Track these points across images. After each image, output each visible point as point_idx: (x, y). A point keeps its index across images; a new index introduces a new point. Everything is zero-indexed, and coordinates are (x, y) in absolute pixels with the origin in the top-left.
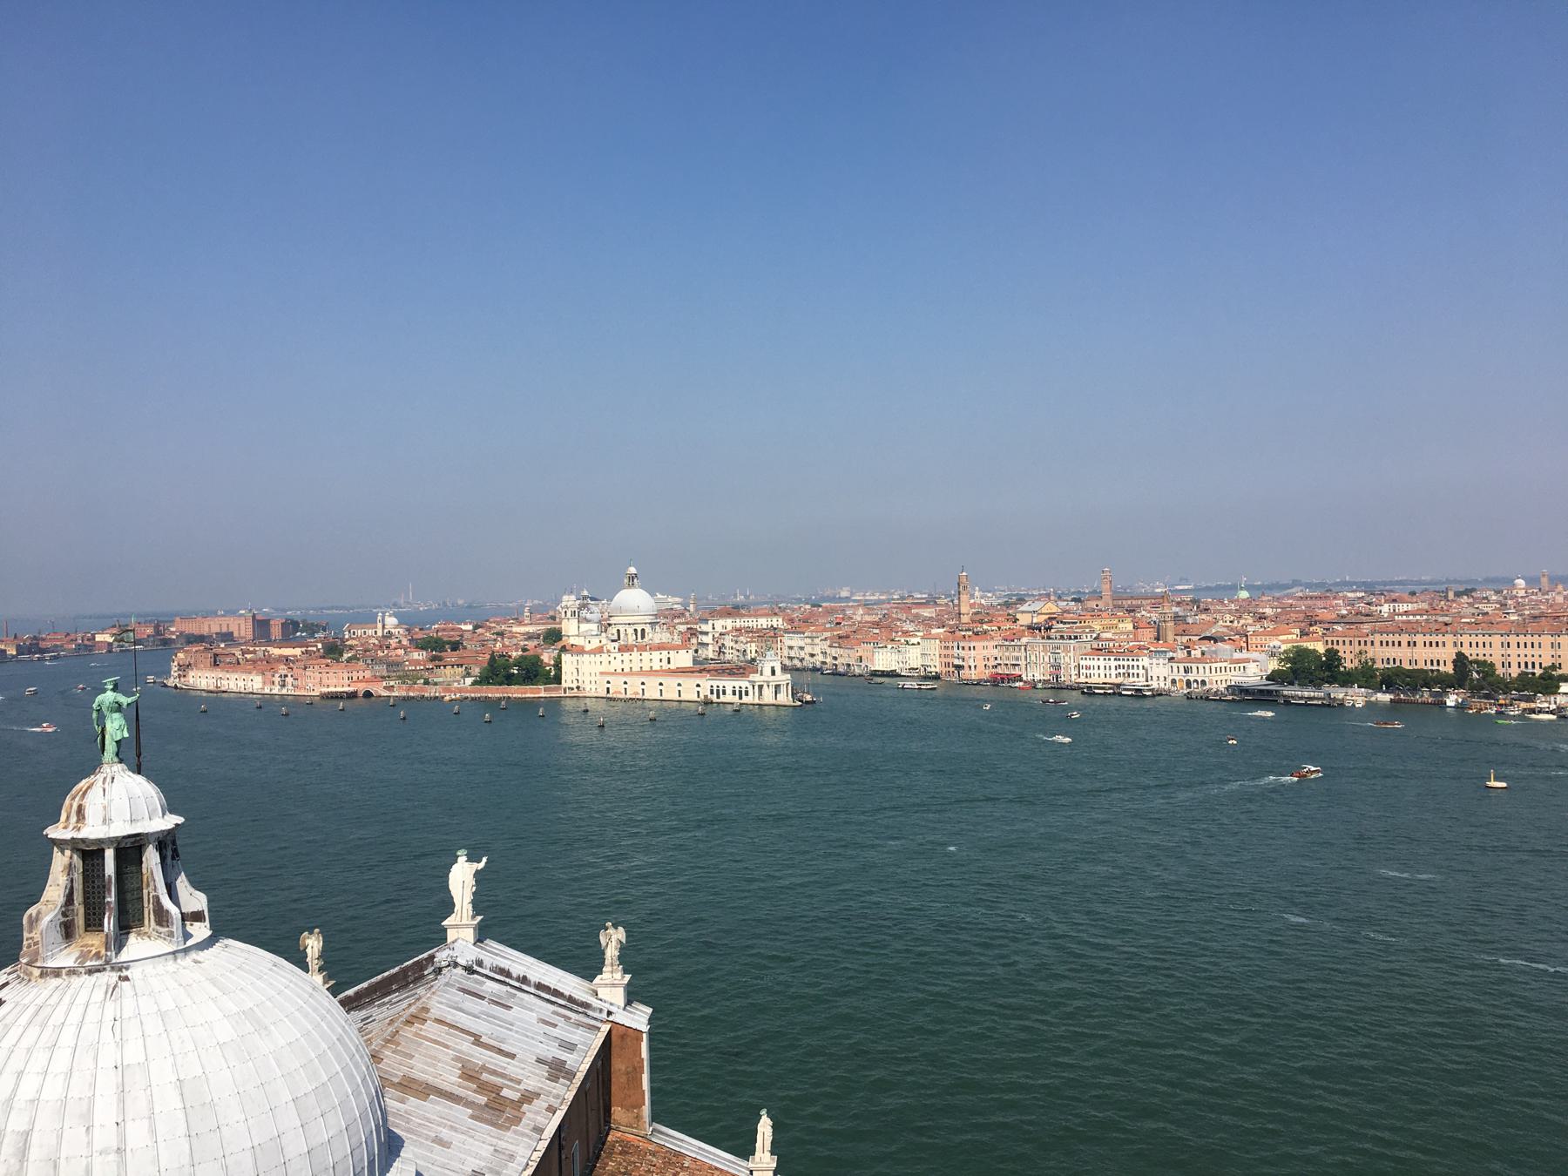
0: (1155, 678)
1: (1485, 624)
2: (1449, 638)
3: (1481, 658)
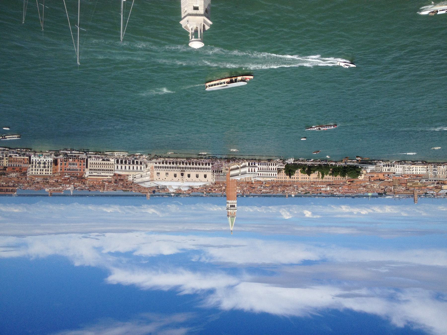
0: (400, 167)
1: (303, 184)
2: (312, 180)
3: (304, 175)
